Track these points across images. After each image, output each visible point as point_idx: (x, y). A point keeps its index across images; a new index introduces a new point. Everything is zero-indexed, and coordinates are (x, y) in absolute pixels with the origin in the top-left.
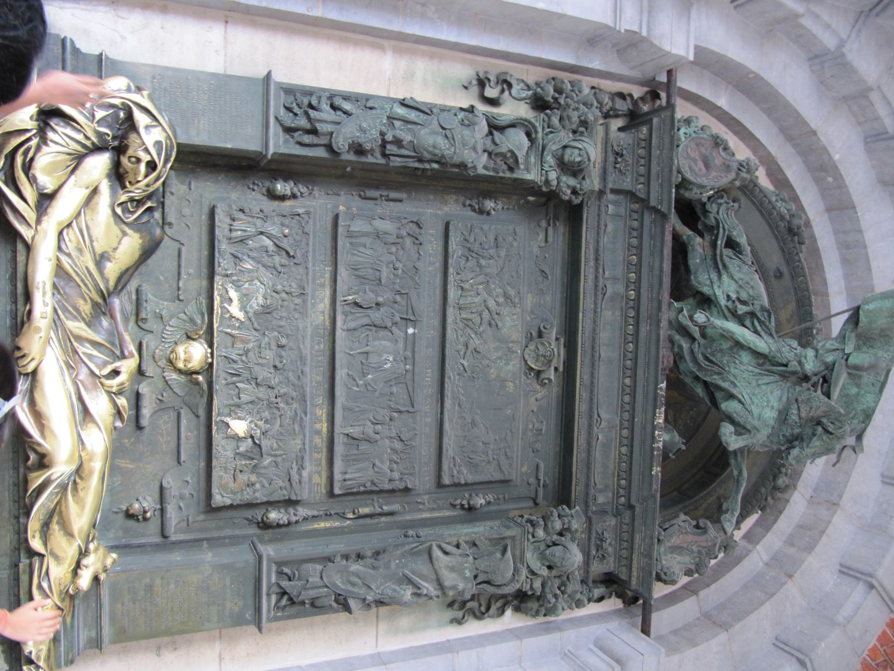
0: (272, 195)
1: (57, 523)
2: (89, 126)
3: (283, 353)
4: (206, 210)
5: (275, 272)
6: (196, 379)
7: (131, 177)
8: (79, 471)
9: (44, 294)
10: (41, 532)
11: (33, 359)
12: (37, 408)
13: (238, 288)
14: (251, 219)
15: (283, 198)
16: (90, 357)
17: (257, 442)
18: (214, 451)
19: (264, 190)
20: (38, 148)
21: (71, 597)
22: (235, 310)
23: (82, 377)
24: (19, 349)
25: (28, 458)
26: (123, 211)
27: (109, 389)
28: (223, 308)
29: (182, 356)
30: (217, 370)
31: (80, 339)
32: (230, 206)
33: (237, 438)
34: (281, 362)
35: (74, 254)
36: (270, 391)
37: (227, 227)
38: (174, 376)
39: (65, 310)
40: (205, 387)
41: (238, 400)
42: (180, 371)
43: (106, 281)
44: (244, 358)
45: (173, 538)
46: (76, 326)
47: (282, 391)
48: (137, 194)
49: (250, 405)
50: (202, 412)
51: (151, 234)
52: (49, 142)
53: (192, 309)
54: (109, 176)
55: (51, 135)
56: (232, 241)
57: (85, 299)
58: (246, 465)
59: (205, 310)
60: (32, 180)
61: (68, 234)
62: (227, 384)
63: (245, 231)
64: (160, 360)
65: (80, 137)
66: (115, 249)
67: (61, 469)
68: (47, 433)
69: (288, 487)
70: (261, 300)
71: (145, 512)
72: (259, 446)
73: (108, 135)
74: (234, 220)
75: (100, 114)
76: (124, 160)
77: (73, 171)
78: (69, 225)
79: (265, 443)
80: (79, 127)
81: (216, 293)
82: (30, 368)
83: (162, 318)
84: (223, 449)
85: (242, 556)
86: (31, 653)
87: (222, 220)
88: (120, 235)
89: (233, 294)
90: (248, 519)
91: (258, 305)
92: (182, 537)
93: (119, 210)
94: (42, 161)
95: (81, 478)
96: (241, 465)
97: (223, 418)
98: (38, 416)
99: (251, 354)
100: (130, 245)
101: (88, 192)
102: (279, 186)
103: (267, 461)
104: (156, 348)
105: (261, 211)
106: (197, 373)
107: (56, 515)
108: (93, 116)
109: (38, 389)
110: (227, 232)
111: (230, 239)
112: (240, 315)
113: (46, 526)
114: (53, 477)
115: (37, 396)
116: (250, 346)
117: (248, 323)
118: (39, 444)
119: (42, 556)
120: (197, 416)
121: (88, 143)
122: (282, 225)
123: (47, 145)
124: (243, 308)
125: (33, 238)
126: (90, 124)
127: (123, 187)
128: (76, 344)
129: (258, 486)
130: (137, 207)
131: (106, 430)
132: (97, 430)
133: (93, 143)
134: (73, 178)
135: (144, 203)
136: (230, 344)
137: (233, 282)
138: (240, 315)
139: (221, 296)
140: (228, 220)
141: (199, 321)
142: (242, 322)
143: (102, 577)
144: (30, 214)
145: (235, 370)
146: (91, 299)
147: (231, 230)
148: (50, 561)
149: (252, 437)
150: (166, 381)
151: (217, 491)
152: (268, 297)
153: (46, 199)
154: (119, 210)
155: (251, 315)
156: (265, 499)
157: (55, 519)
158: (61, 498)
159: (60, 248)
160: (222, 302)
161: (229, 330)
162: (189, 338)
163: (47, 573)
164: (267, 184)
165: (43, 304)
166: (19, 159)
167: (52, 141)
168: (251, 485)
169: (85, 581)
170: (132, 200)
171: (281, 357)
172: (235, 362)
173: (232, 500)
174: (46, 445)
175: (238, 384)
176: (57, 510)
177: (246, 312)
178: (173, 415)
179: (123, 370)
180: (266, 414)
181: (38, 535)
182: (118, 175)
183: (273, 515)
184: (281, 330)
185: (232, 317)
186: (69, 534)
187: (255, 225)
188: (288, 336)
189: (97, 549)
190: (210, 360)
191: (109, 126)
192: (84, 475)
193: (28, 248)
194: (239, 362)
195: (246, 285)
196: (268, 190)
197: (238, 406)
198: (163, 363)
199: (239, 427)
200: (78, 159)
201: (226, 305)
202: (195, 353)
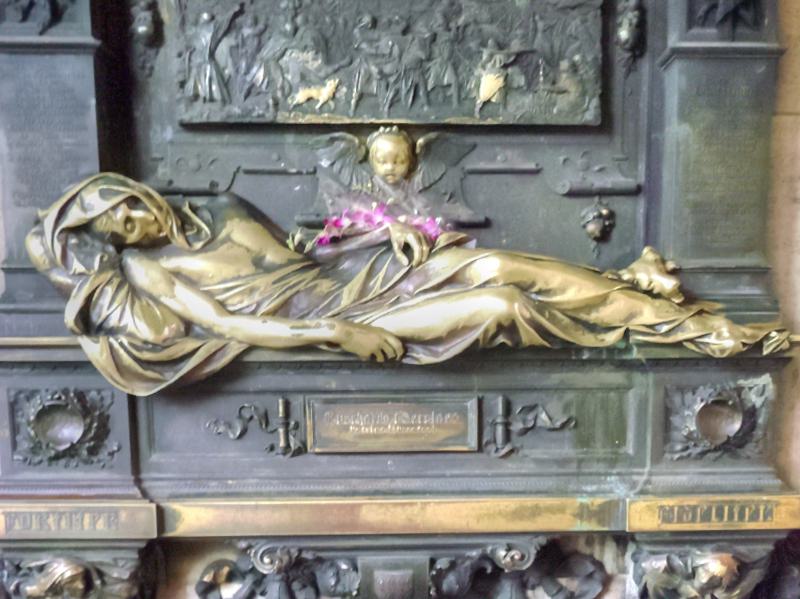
0: (156, 38)
1: (588, 314)
2: (95, 278)
3: (384, 20)
5: (267, 35)
6: (422, 147)
7: (153, 229)
8: (523, 288)
10: (600, 333)
11: (386, 341)
12: (444, 335)
13: (291, 90)
14: (194, 71)
15: (158, 24)
16: (386, 280)
17: (512, 59)
18: (522, 122)
19: (151, 52)
20: (130, 335)
21: (689, 298)
22: (323, 94)
23: (411, 288)
24: (373, 356)
25: (503, 344)
26: (199, 240)
29: (389, 166)
30: (410, 118)
31: (364, 290)
32: (179, 101)
33: (507, 89)
34: (397, 23)
35: (257, 297)
36: (439, 40)
37: (208, 105)
39: (328, 308)
40: (432, 135)
41: (453, 86)
43: (291, 262)
44: (392, 80)
46: (347, 296)
47: (440, 20)
48: (173, 224)
49: (460, 69)
50: (470, 140)
51: (227, 206)
52: (122, 325)
54: (155, 259)
55: (113, 322)
56: (226, 98)
58: (545, 75)
59: (327, 137)
61: (233, 305)
62: (429, 103)
63: (211, 80)
65: (110, 290)
66: (248, 250)
67: (520, 310)
68: (478, 319)
69: (584, 10)
70: (310, 55)
72: (519, 55)
73: (102, 258)
74: (196, 97)
75: (77, 266)
76: (132, 238)
78: (222, 304)
79: (516, 46)
80: (98, 291)
81: (301, 121)
82: (396, 344)
84: (523, 107)
85: (676, 79)
86: (744, 344)
87: (199, 113)
88: (229, 244)
89: (301, 96)
91: (315, 59)
93: (198, 245)
94: (145, 332)
95: (533, 284)
96: (544, 82)
97: (477, 109)
98: (454, 333)
99: (387, 69)
100: (240, 232)
101: (177, 282)
102: (142, 29)
103: (539, 42)
105: (180, 55)
106: (413, 146)
107: (577, 317)
108: (81, 274)
109: (422, 335)
110: (215, 107)
112: (331, 84)
113: (593, 328)
114: (528, 315)
115: (430, 336)
116: (374, 70)
117: (341, 73)
118: (486, 331)
120: (474, 146)
121: (116, 281)
122: (196, 23)
123: (126, 326)
124: (322, 82)
126: (92, 278)
127: (166, 241)
128: (370, 297)
129: (577, 58)
130: (192, 224)
131: (472, 257)
132: (474, 266)
134: (163, 299)
135: (186, 215)
136: (373, 100)
137: (286, 97)
138: (331, 84)
139: (305, 112)
140: (199, 104)
141: (343, 145)
142: (340, 83)
143: (671, 265)
144: (212, 345)
145: (409, 91)
146: (315, 279)
148: (633, 325)
149: (505, 66)
151: (579, 118)
152: (303, 44)
153: (188, 327)
154: (198, 245)
155: (330, 70)
156: (598, 45)
157: (583, 316)
159: (253, 313)
160: (314, 112)
161: (353, 102)
162: (366, 158)
163: (651, 326)
164: (140, 47)
165: (322, 329)
166: (147, 356)
167: (120, 320)
168: (574, 68)
169: (668, 284)
170: (182, 229)
171: (390, 22)
172: (397, 92)
173: (593, 96)
174: (488, 322)
175: (429, 88)
177: (327, 77)
178: (472, 178)
179: (402, 240)
180: (473, 45)
181: (602, 336)
182: (152, 246)
183: (624, 34)
184: (351, 24)
185: (333, 97)
186: (603, 300)
187: (199, 66)
188: (359, 13)
190: (395, 128)
191: (92, 255)
192: (529, 282)
193: (252, 348)
194: (397, 86)
195: (289, 77)
197: (460, 87)
199: (488, 84)
200: (135, 292)
202: (384, 147)
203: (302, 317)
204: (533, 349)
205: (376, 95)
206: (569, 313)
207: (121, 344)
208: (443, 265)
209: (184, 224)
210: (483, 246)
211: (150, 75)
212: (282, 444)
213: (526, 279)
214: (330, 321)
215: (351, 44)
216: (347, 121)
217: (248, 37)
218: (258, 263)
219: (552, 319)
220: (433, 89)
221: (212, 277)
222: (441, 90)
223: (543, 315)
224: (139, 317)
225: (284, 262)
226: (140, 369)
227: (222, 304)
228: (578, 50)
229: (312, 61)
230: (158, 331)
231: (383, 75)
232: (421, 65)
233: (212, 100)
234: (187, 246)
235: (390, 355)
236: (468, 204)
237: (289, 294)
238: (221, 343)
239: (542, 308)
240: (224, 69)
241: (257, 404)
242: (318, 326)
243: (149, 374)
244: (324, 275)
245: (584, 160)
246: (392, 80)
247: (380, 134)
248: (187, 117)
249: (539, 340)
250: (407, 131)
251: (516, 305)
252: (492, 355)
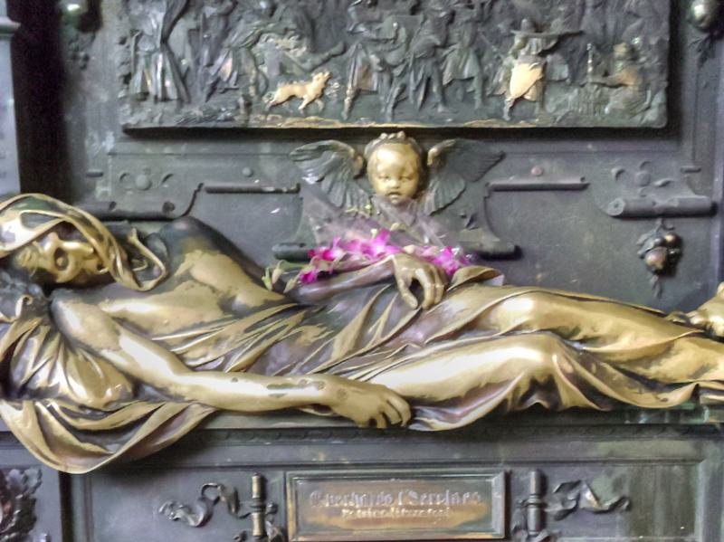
1: (647, 367)
4: (133, 146)
8: (564, 335)
9: (286, 386)
11: (388, 402)
13: (270, 86)
23: (420, 336)
24: (372, 422)
27: (440, 293)
29: (392, 183)
31: (360, 339)
33: (545, 83)
35: (224, 349)
39: (315, 361)
40: (448, 143)
44: (397, 72)
46: (340, 346)
50: (496, 148)
52: (51, 385)
55: (41, 381)
59: (313, 146)
62: (445, 101)
65: (36, 342)
74: (145, 95)
79: (557, 27)
82: (402, 406)
84: (565, 106)
89: (279, 94)
93: (149, 284)
94: (81, 393)
95: (577, 330)
98: (475, 392)
99: (392, 58)
100: (203, 267)
101: (122, 330)
106: (424, 157)
107: (634, 371)
110: (170, 107)
111: (180, 100)
112: (318, 79)
114: (569, 369)
117: (332, 64)
118: (517, 389)
120: (502, 156)
121: (44, 330)
123: (57, 386)
124: (307, 75)
130: (142, 257)
138: (318, 79)
140: (148, 105)
141: (333, 156)
144: (168, 409)
147: (165, 99)
149: (543, 54)
153: (137, 387)
154: (149, 284)
155: (318, 59)
157: (640, 370)
159: (220, 369)
160: (297, 115)
165: (307, 389)
166: (84, 424)
170: (129, 264)
172: (404, 88)
177: (314, 69)
179: (410, 276)
181: (663, 396)
182: (91, 285)
185: (322, 96)
186: (666, 350)
189: (704, 314)
192: (571, 328)
195: (265, 69)
199: (521, 77)
200: (69, 345)
202: (386, 158)
203: (281, 374)
204: (576, 411)
206: (623, 367)
207: (51, 410)
209: (132, 256)
210: (511, 282)
211: (84, 67)
212: (256, 531)
213: (568, 325)
214: (319, 378)
215: (345, 26)
216: (339, 125)
218: (227, 307)
219: (601, 374)
220: (450, 84)
221: (167, 324)
222: (459, 84)
223: (589, 369)
224: (72, 376)
225: (259, 304)
226: (76, 442)
227: (180, 358)
228: (639, 30)
229: (296, 50)
230: (99, 393)
231: (386, 67)
233: (165, 99)
234: (134, 285)
235: (394, 420)
236: (493, 230)
237: (265, 344)
238: (178, 407)
239: (587, 360)
241: (224, 482)
242: (303, 385)
243: (88, 446)
244: (310, 320)
245: (645, 172)
246: (397, 72)
247: (383, 142)
248: (132, 121)
249: (582, 400)
251: (555, 358)
252: (524, 418)
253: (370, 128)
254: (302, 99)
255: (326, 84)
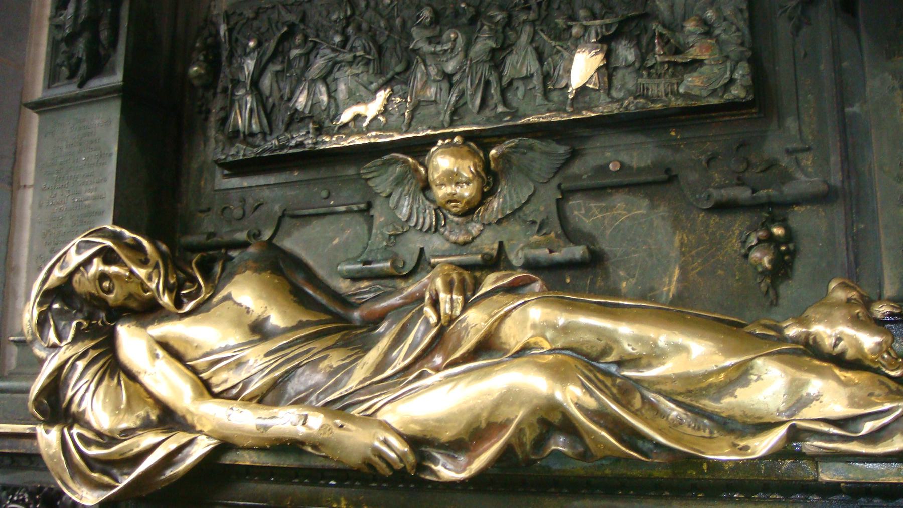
1: (718, 400)
6: (496, 160)
11: (386, 442)
17: (613, 29)
22: (371, 109)
28: (369, 129)
30: (478, 124)
31: (381, 366)
33: (607, 70)
38: (495, 204)
41: (535, 78)
42: (484, 196)
43: (301, 326)
44: (455, 78)
45: (836, 179)
53: (382, 183)
54: (144, 326)
57: (325, 358)
59: (378, 162)
60: (128, 433)
61: (218, 385)
63: (251, 110)
64: (468, 232)
65: (81, 364)
71: (771, 239)
73: (79, 325)
77: (133, 377)
82: (405, 448)
83: (396, 236)
87: (240, 151)
89: (346, 116)
90: (797, 29)
92: (835, 159)
93: (188, 307)
99: (450, 67)
104: (448, 240)
106: (486, 163)
112: (382, 95)
118: (519, 431)
119: (795, 434)
121: (93, 354)
123: (84, 412)
125: (209, 436)
126: (63, 349)
133: (94, 347)
136: (432, 109)
141: (398, 169)
150: (507, 217)
157: (708, 404)
158: (659, 392)
159: (235, 398)
166: (93, 452)
168: (708, 30)
172: (462, 95)
176: (688, 400)
180: (561, 22)
182: (146, 311)
185: (385, 112)
186: (741, 375)
196: (206, 87)
198: (475, 228)
201: (365, 125)
202: (449, 168)
205: (435, 102)
206: (680, 398)
208: (476, 320)
216: (397, 137)
217: (295, 58)
218: (259, 330)
224: (98, 400)
227: (207, 385)
232: (496, 59)
240: (267, 98)
250: (477, 142)
253: (427, 136)
254: (366, 117)
255: (388, 100)
